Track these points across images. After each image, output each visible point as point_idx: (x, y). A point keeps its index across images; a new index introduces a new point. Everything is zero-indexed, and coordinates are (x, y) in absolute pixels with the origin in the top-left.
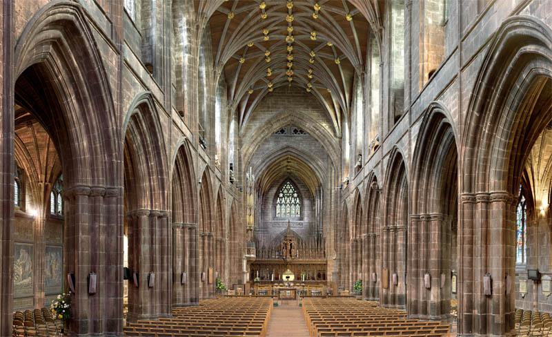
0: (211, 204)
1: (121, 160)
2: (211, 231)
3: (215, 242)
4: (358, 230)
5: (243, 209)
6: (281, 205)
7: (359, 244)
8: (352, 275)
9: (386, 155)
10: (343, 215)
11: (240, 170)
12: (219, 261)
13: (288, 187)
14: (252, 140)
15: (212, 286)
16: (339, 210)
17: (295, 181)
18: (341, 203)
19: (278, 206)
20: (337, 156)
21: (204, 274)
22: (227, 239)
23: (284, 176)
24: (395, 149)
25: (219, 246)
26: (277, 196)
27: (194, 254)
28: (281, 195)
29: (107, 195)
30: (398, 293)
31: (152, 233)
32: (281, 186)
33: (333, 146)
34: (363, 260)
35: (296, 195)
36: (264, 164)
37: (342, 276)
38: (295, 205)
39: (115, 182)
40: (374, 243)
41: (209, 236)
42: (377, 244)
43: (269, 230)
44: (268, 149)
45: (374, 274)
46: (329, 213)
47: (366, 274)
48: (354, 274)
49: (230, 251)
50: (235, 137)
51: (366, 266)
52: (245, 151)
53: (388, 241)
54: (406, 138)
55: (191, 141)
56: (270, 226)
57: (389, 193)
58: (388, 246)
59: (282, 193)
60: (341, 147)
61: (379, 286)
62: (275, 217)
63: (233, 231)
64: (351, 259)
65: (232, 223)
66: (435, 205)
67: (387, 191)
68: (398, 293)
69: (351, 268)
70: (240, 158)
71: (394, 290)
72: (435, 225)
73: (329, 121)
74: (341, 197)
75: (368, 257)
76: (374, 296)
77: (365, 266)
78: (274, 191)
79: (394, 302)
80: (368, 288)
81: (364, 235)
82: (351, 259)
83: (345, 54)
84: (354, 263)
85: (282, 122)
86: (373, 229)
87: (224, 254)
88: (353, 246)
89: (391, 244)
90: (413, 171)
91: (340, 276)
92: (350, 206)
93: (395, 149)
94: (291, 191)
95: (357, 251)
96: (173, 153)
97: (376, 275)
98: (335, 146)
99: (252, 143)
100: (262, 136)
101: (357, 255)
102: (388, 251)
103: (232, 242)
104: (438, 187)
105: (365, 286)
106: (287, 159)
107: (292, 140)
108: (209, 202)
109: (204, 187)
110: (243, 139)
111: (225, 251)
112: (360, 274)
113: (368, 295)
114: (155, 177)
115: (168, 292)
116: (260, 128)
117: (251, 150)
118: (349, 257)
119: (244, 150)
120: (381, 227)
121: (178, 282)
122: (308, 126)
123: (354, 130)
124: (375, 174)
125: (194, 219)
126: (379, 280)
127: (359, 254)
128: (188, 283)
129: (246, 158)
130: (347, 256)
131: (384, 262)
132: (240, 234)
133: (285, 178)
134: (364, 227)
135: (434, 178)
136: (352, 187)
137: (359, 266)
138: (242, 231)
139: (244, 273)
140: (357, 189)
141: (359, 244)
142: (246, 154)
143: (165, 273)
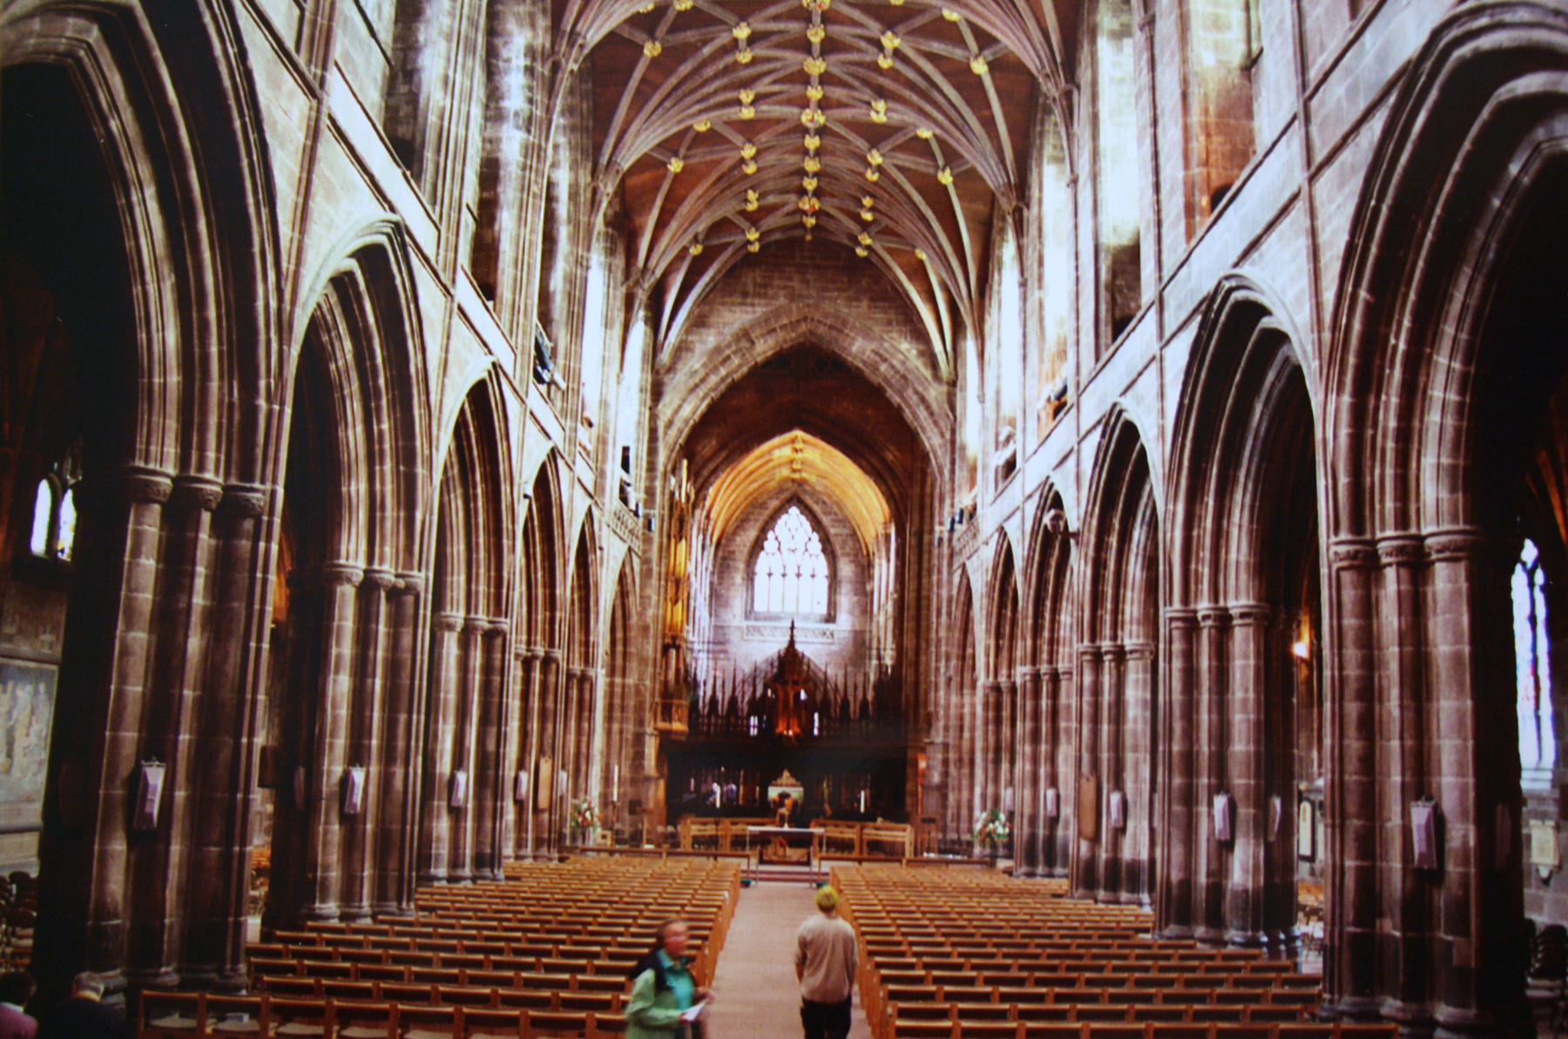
0: (559, 562)
2: (552, 645)
3: (563, 679)
4: (1005, 654)
5: (654, 581)
7: (1006, 699)
8: (984, 796)
9: (1089, 432)
10: (957, 613)
11: (651, 467)
12: (572, 738)
14: (692, 383)
15: (546, 816)
16: (944, 594)
17: (817, 508)
18: (950, 574)
20: (942, 435)
21: (524, 776)
22: (600, 675)
23: (781, 490)
24: (1115, 412)
25: (574, 693)
26: (758, 546)
27: (494, 711)
30: (1127, 854)
31: (364, 638)
33: (928, 407)
34: (1019, 748)
37: (952, 798)
40: (1054, 695)
41: (548, 661)
42: (1063, 700)
43: (732, 649)
45: (1051, 793)
46: (913, 604)
47: (1027, 793)
48: (990, 790)
49: (610, 708)
50: (643, 369)
51: (1028, 767)
53: (1096, 690)
54: (1150, 378)
55: (509, 369)
56: (734, 637)
57: (1101, 546)
58: (1096, 706)
60: (953, 408)
61: (1067, 832)
62: (749, 613)
63: (619, 648)
64: (979, 745)
65: (619, 623)
66: (1243, 577)
67: (1093, 539)
68: (1127, 854)
69: (979, 772)
70: (653, 432)
71: (1116, 846)
72: (1246, 639)
73: (920, 335)
74: (951, 556)
75: (1035, 737)
76: (1050, 862)
77: (1023, 767)
78: (751, 534)
79: (1113, 885)
80: (1033, 836)
81: (1022, 672)
82: (979, 745)
84: (991, 756)
85: (781, 335)
86: (1051, 653)
87: (591, 719)
88: (986, 706)
89: (1106, 698)
90: (1171, 477)
91: (945, 797)
92: (980, 581)
93: (1115, 412)
95: (998, 721)
96: (451, 401)
97: (1058, 797)
98: (935, 407)
100: (723, 371)
101: (998, 732)
102: (1096, 720)
103: (618, 680)
104: (1251, 522)
105: (1022, 831)
106: (793, 441)
108: (549, 557)
109: (539, 511)
110: (666, 379)
111: (591, 710)
112: (1009, 791)
113: (1031, 860)
114: (388, 466)
116: (718, 350)
117: (687, 410)
118: (972, 739)
119: (665, 410)
120: (1071, 649)
121: (440, 804)
122: (858, 349)
123: (994, 363)
124: (1057, 487)
125: (499, 605)
126: (1067, 811)
127: (1006, 730)
128: (470, 805)
129: (673, 432)
130: (966, 735)
131: (1086, 757)
132: (643, 660)
133: (786, 495)
134: (1023, 646)
135: (1238, 496)
136: (987, 523)
137: (1005, 766)
138: (651, 648)
139: (648, 779)
140: (1002, 532)
141: (1006, 699)
142: (670, 424)
143: (399, 771)
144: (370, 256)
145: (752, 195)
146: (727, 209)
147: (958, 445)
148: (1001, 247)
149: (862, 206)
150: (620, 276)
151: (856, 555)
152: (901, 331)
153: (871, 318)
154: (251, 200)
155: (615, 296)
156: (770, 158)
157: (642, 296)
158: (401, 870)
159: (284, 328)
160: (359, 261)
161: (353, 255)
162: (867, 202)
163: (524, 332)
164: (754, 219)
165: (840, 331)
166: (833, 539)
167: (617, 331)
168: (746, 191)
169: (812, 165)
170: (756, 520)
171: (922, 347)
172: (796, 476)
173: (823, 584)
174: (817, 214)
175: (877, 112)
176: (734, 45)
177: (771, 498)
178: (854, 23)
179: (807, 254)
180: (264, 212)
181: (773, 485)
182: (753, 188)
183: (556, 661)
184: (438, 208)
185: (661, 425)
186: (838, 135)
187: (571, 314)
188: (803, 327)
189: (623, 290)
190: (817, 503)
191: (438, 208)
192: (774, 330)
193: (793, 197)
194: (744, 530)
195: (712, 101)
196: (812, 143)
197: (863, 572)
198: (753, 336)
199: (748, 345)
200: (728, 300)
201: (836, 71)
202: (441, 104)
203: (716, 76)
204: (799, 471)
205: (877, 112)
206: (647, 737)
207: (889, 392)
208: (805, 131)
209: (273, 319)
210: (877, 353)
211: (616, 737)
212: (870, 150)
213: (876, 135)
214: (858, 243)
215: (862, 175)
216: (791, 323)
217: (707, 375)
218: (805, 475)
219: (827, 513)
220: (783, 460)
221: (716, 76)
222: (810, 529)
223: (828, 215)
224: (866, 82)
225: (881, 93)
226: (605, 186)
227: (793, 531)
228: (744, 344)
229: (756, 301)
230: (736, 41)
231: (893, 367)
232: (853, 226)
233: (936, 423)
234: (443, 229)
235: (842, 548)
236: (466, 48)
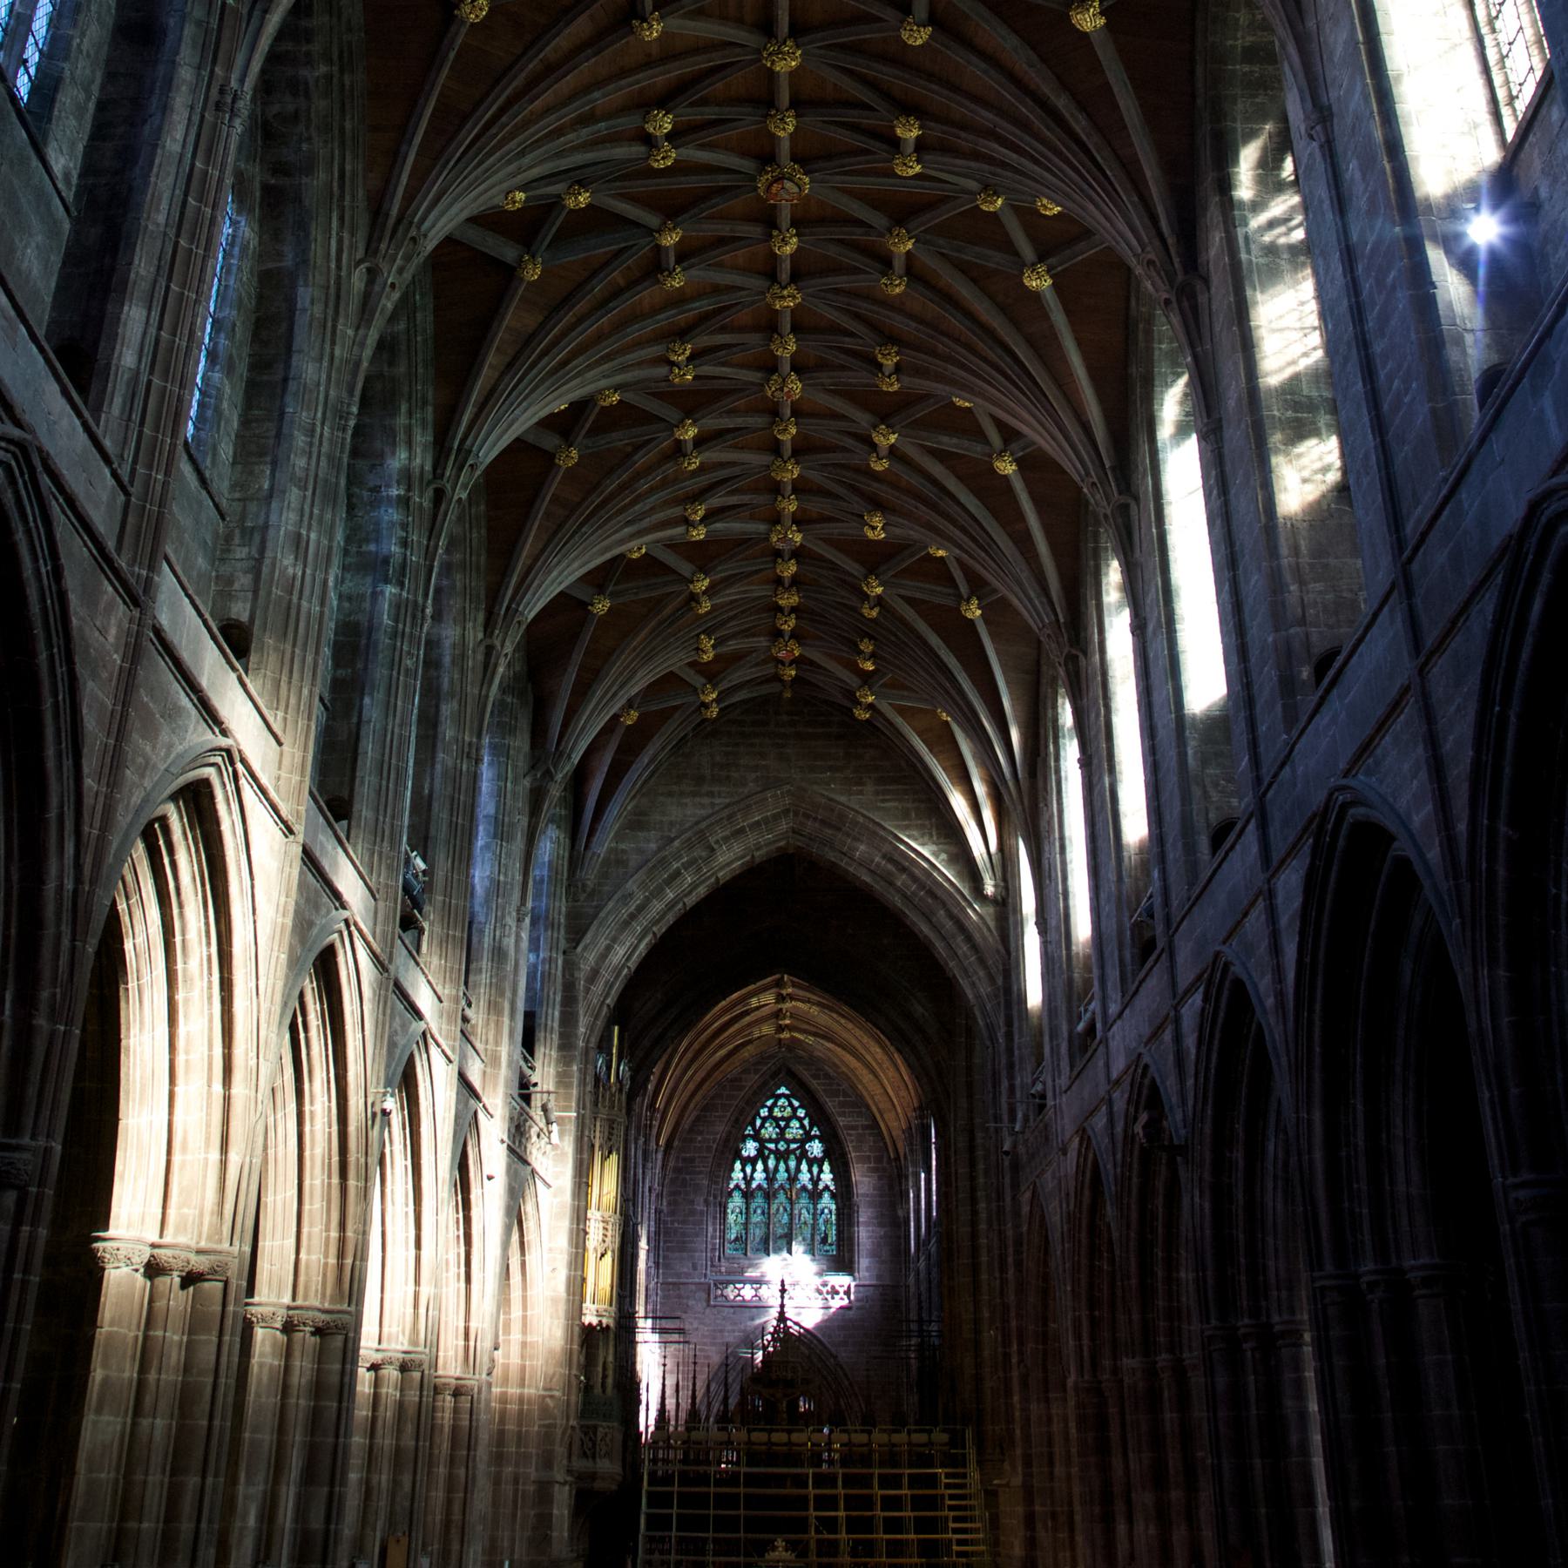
14: (625, 913)
17: (814, 1084)
19: (737, 1201)
20: (992, 979)
23: (762, 1059)
28: (750, 1148)
33: (969, 938)
35: (816, 1148)
38: (815, 1195)
52: (592, 957)
59: (756, 1137)
73: (951, 833)
83: (996, 583)
85: (752, 839)
94: (794, 1130)
99: (626, 924)
117: (620, 952)
142: (594, 974)
145: (707, 643)
146: (674, 661)
147: (1015, 995)
148: (1055, 707)
149: (860, 652)
150: (522, 763)
151: (879, 1160)
152: (922, 827)
153: (879, 809)
155: (514, 793)
156: (731, 594)
157: (555, 791)
162: (867, 646)
164: (711, 673)
165: (839, 829)
166: (843, 1134)
167: (519, 844)
168: (698, 635)
169: (789, 600)
171: (953, 849)
172: (782, 1036)
174: (797, 662)
175: (874, 528)
176: (678, 450)
178: (835, 416)
179: (785, 718)
181: (746, 1053)
182: (709, 634)
186: (821, 558)
187: (453, 827)
188: (784, 826)
189: (527, 782)
190: (816, 1077)
192: (741, 831)
193: (763, 642)
195: (646, 523)
196: (790, 569)
197: (891, 1187)
198: (712, 840)
199: (704, 854)
200: (675, 788)
201: (815, 476)
202: (290, 571)
203: (652, 490)
205: (874, 528)
206: (557, 1487)
207: (913, 917)
208: (778, 554)
210: (891, 860)
212: (866, 577)
213: (876, 558)
214: (857, 703)
215: (856, 610)
216: (766, 821)
217: (647, 901)
218: (796, 1035)
220: (765, 1011)
221: (652, 490)
222: (806, 1122)
223: (812, 663)
224: (853, 489)
225: (878, 505)
226: (502, 646)
227: (782, 1124)
228: (700, 852)
229: (716, 789)
230: (679, 442)
231: (915, 879)
232: (852, 680)
233: (982, 961)
235: (856, 1149)
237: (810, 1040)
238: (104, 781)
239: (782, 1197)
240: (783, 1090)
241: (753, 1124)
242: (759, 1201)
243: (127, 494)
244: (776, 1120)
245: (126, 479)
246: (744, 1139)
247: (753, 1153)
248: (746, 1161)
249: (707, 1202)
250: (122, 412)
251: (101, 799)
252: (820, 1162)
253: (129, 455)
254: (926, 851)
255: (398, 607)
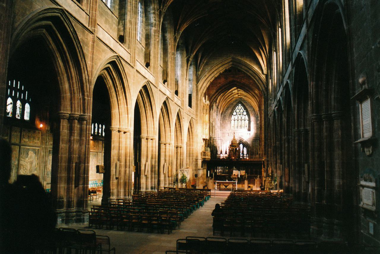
1: (90, 98)
6: (234, 120)
13: (240, 108)
15: (171, 178)
17: (245, 104)
19: (233, 122)
23: (236, 100)
26: (231, 114)
28: (234, 113)
29: (81, 120)
32: (234, 108)
35: (245, 113)
36: (217, 93)
38: (245, 120)
39: (86, 111)
44: (220, 83)
59: (236, 112)
78: (230, 111)
85: (226, 66)
107: (237, 77)
115: (129, 182)
119: (200, 85)
129: (202, 90)
139: (199, 169)
144: (113, 63)
151: (255, 115)
154: (80, 58)
158: (129, 190)
159: (90, 82)
160: (110, 64)
161: (108, 63)
163: (157, 73)
166: (249, 111)
170: (231, 108)
172: (240, 96)
173: (247, 122)
177: (234, 102)
180: (83, 60)
181: (234, 99)
183: (172, 144)
184: (130, 50)
185: (199, 88)
190: (245, 103)
191: (130, 50)
194: (228, 110)
204: (240, 95)
209: (87, 81)
211: (191, 160)
219: (248, 105)
220: (236, 93)
222: (243, 110)
234: (131, 54)
236: (134, 13)
237: (243, 97)
238: (91, 62)
239: (240, 120)
240: (240, 105)
241: (235, 110)
242: (236, 121)
243: (89, 16)
244: (239, 109)
245: (88, 14)
246: (234, 112)
247: (235, 114)
248: (234, 115)
249: (228, 121)
250: (87, 2)
251: (91, 65)
252: (246, 115)
253: (89, 9)
254: (256, 68)
255: (155, 31)
